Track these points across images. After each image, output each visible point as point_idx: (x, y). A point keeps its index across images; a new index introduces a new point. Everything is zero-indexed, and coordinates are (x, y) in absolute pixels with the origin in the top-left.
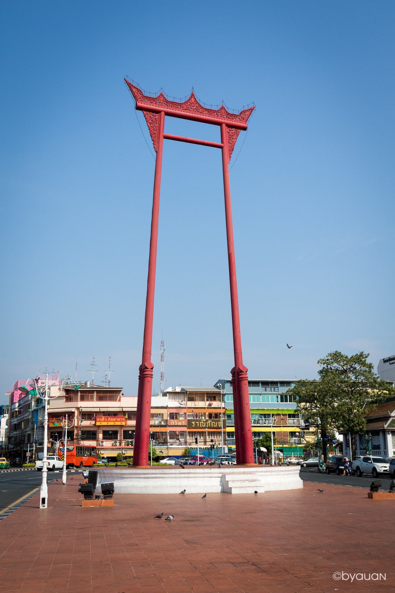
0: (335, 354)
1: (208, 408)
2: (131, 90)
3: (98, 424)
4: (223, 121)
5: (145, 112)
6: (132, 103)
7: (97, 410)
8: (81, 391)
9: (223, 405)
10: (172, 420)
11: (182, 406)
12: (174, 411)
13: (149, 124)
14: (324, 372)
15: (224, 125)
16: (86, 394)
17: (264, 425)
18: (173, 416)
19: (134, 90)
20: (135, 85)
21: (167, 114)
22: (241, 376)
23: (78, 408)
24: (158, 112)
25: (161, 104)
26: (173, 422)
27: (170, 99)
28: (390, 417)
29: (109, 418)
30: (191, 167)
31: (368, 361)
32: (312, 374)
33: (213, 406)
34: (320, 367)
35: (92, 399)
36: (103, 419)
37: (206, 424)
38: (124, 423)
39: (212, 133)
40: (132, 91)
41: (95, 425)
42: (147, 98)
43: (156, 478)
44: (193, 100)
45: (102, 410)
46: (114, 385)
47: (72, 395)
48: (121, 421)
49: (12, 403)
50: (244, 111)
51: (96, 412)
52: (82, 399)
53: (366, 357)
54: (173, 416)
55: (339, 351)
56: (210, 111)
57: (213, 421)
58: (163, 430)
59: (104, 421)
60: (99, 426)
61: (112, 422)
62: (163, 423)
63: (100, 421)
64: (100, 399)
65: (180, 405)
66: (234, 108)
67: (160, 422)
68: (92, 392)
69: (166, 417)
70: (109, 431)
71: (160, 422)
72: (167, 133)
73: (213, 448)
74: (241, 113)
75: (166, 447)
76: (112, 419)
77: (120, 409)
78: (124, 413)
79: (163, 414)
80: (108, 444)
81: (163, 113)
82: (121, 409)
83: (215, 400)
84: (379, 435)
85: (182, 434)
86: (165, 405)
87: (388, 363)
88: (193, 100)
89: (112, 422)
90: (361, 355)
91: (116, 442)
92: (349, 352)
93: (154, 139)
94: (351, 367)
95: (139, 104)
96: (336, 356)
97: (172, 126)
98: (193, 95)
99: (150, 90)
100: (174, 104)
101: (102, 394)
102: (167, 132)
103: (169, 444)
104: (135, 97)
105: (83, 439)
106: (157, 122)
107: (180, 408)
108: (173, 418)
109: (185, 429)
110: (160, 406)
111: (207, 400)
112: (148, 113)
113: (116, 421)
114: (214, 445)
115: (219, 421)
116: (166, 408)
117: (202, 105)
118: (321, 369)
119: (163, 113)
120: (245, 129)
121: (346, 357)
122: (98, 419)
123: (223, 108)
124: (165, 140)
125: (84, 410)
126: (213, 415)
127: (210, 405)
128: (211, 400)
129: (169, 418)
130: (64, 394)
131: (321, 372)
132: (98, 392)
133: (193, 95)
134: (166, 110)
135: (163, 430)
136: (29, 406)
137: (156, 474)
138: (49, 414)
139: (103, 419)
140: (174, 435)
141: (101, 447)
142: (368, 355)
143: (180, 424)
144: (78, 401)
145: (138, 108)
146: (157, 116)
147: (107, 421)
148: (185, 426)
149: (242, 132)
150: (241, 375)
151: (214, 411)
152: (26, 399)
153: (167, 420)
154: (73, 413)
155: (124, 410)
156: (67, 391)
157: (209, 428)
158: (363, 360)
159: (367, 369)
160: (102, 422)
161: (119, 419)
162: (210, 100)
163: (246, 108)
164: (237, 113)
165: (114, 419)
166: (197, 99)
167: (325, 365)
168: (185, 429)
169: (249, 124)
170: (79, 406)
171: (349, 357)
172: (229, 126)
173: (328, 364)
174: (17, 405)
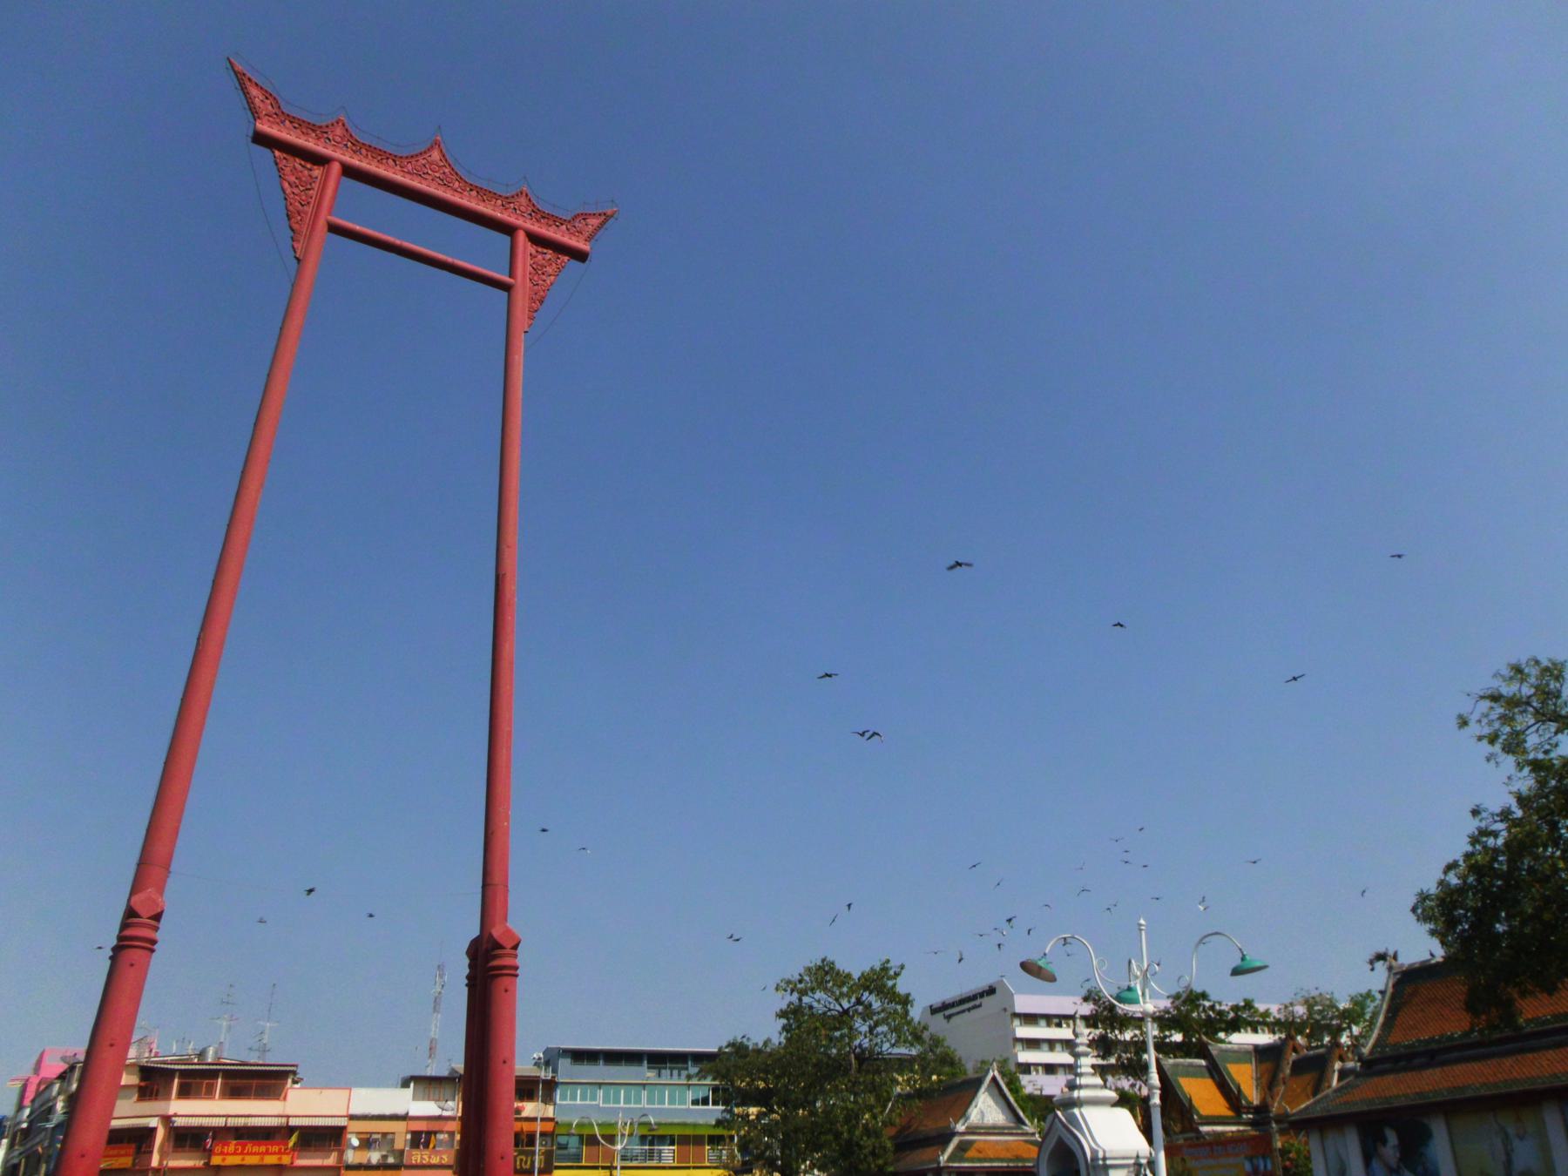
0: (819, 968)
2: (244, 89)
3: (216, 1160)
4: (520, 222)
7: (220, 1122)
8: (184, 1074)
9: (550, 1111)
10: (414, 1152)
11: (446, 1114)
12: (422, 1126)
13: (286, 185)
14: (792, 1015)
15: (521, 236)
16: (195, 1081)
17: (649, 1163)
18: (420, 1139)
19: (254, 92)
21: (349, 172)
23: (167, 1119)
24: (321, 160)
26: (418, 1156)
28: (953, 1134)
31: (902, 987)
32: (766, 1031)
33: (524, 1114)
34: (785, 1000)
35: (209, 1094)
36: (232, 1148)
38: (286, 1160)
40: (246, 93)
44: (436, 155)
45: (232, 1122)
46: (275, 1059)
48: (280, 1152)
49: (20, 1107)
52: (185, 1093)
53: (897, 975)
55: (830, 958)
57: (521, 1153)
59: (235, 1153)
62: (391, 1160)
63: (222, 1153)
64: (234, 1093)
68: (212, 1074)
71: (385, 1157)
76: (255, 1149)
77: (284, 1120)
78: (291, 1130)
81: (336, 168)
82: (284, 1120)
86: (401, 1111)
87: (940, 1016)
88: (436, 155)
90: (884, 969)
92: (855, 965)
93: (295, 226)
94: (859, 1002)
95: (265, 127)
96: (825, 975)
106: (315, 186)
107: (440, 1118)
110: (388, 1112)
113: (267, 1153)
115: (533, 1153)
116: (405, 1118)
118: (784, 1007)
120: (581, 256)
121: (849, 976)
122: (218, 1149)
125: (179, 1122)
126: (524, 1137)
131: (782, 1014)
132: (228, 1074)
136: (51, 1110)
142: (902, 967)
143: (435, 1160)
144: (168, 1097)
145: (260, 139)
146: (317, 172)
150: (496, 957)
151: (526, 1127)
152: (46, 1096)
153: (402, 1152)
154: (152, 1131)
155: (293, 1122)
158: (890, 983)
159: (899, 1007)
161: (275, 1149)
165: (263, 1149)
167: (796, 995)
170: (171, 1112)
171: (856, 975)
172: (535, 239)
173: (803, 993)
174: (27, 1112)
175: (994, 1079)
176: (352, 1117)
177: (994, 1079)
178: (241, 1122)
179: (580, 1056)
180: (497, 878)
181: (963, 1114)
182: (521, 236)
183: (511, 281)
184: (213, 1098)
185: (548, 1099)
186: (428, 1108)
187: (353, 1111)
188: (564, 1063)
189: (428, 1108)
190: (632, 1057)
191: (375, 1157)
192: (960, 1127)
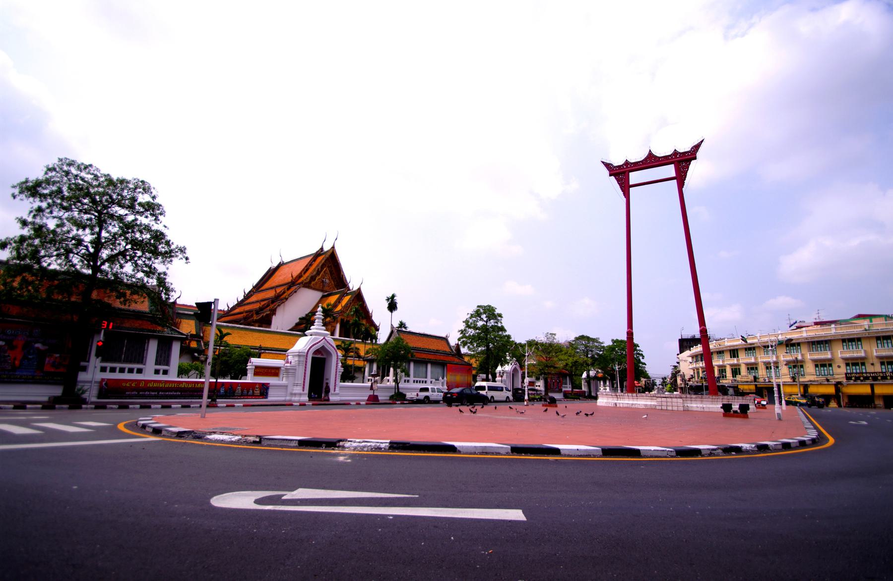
6: (607, 172)
20: (608, 162)
24: (624, 173)
30: (654, 198)
39: (670, 170)
66: (684, 147)
72: (631, 183)
97: (635, 177)
99: (618, 161)
100: (636, 164)
120: (695, 158)
145: (610, 175)
149: (693, 162)
162: (662, 151)
163: (696, 143)
164: (688, 149)
169: (698, 154)
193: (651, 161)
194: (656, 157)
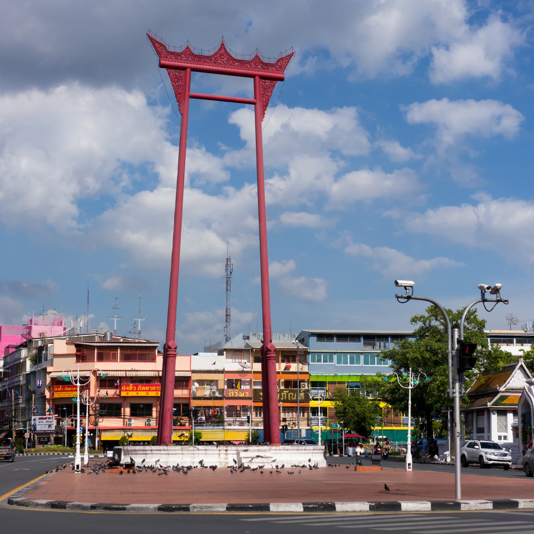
1: (283, 373)
3: (124, 394)
4: (256, 73)
5: (169, 70)
6: (155, 59)
7: (123, 374)
8: (98, 347)
9: (306, 369)
11: (245, 370)
15: (257, 78)
16: (105, 353)
18: (231, 384)
22: (268, 356)
23: (95, 372)
24: (184, 69)
25: (187, 61)
26: (232, 393)
27: (196, 52)
28: (498, 392)
29: (140, 386)
33: (292, 370)
35: (114, 359)
36: (131, 388)
37: (281, 396)
41: (119, 395)
42: (172, 53)
43: (176, 454)
44: (223, 50)
45: (129, 374)
47: (86, 352)
50: (282, 59)
51: (121, 378)
52: (101, 358)
54: (231, 384)
56: (242, 63)
57: (290, 391)
58: (217, 403)
59: (133, 390)
60: (125, 398)
61: (143, 392)
62: (217, 394)
63: (126, 390)
64: (126, 358)
65: (241, 369)
66: (270, 57)
67: (214, 393)
68: (116, 348)
69: (222, 385)
70: (139, 404)
73: (286, 429)
74: (279, 61)
75: (222, 427)
76: (143, 388)
79: (217, 381)
80: (138, 422)
81: (189, 70)
82: (157, 373)
83: (294, 361)
84: (484, 415)
85: (245, 409)
88: (223, 50)
89: (143, 392)
91: (149, 421)
95: (163, 62)
98: (223, 45)
99: (175, 44)
100: (200, 58)
101: (129, 352)
102: (194, 90)
103: (226, 424)
104: (159, 53)
105: (102, 416)
107: (243, 372)
108: (233, 387)
109: (250, 403)
111: (283, 361)
112: (173, 70)
113: (150, 390)
114: (286, 426)
116: (222, 372)
117: (233, 56)
119: (189, 70)
120: (282, 79)
122: (123, 388)
123: (257, 56)
124: (191, 100)
125: (102, 373)
127: (287, 368)
128: (289, 361)
129: (226, 387)
130: (72, 350)
133: (223, 45)
134: (192, 65)
135: (217, 403)
137: (176, 450)
138: (53, 379)
139: (131, 388)
140: (233, 411)
141: (128, 427)
143: (242, 395)
145: (162, 66)
147: (136, 390)
148: (250, 398)
149: (279, 83)
150: (268, 354)
152: (16, 356)
154: (88, 378)
156: (78, 347)
157: (284, 401)
160: (130, 392)
161: (154, 388)
163: (284, 55)
164: (273, 61)
165: (147, 388)
166: (227, 50)
168: (250, 403)
172: (262, 77)
175: (521, 366)
176: (193, 372)
177: (521, 366)
178: (134, 374)
179: (321, 337)
180: (267, 324)
181: (503, 381)
182: (257, 78)
183: (255, 100)
184: (117, 361)
185: (304, 361)
186: (232, 365)
187: (192, 369)
188: (313, 339)
189: (232, 365)
190: (354, 337)
191: (207, 393)
192: (502, 389)
193: (223, 63)
194: (230, 58)
